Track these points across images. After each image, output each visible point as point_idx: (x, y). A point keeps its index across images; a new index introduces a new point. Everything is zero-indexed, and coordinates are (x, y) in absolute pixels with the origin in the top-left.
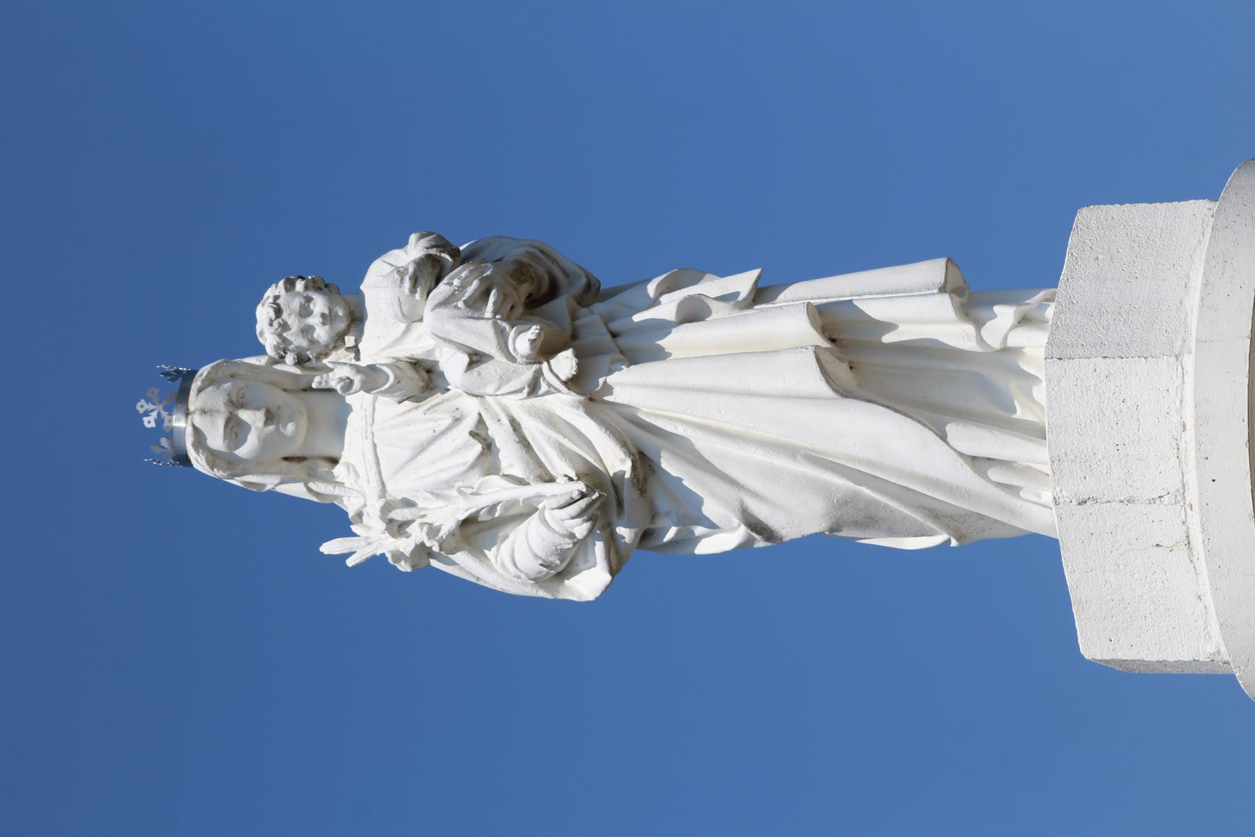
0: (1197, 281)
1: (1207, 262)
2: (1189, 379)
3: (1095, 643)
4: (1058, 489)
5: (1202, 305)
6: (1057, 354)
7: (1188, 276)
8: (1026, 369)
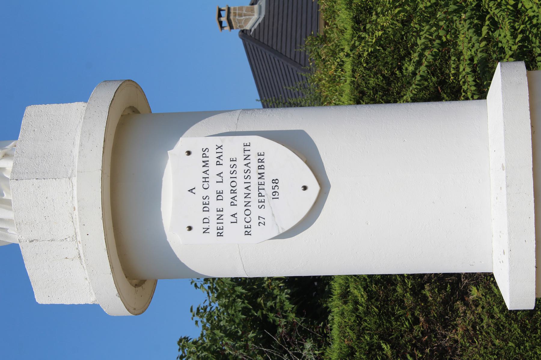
0: (78, 142)
1: (82, 134)
2: (75, 188)
3: (41, 298)
4: (20, 236)
5: (80, 155)
6: (15, 178)
7: (74, 139)
8: (7, 176)
